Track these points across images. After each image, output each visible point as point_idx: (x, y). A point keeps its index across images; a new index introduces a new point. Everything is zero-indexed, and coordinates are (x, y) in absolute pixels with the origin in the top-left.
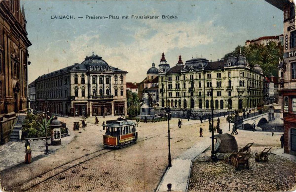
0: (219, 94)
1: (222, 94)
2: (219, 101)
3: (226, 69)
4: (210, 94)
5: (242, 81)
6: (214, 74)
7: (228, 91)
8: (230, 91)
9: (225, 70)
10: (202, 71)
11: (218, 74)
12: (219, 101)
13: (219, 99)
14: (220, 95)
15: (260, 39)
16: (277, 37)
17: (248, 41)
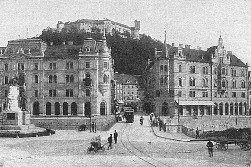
0: (69, 93)
1: (75, 93)
2: (70, 103)
3: (82, 57)
4: (53, 93)
5: (107, 76)
6: (61, 65)
7: (85, 89)
8: (88, 89)
9: (80, 58)
10: (40, 58)
11: (68, 64)
12: (70, 103)
13: (70, 101)
14: (72, 95)
15: (78, 22)
16: (102, 22)
17: (61, 23)
